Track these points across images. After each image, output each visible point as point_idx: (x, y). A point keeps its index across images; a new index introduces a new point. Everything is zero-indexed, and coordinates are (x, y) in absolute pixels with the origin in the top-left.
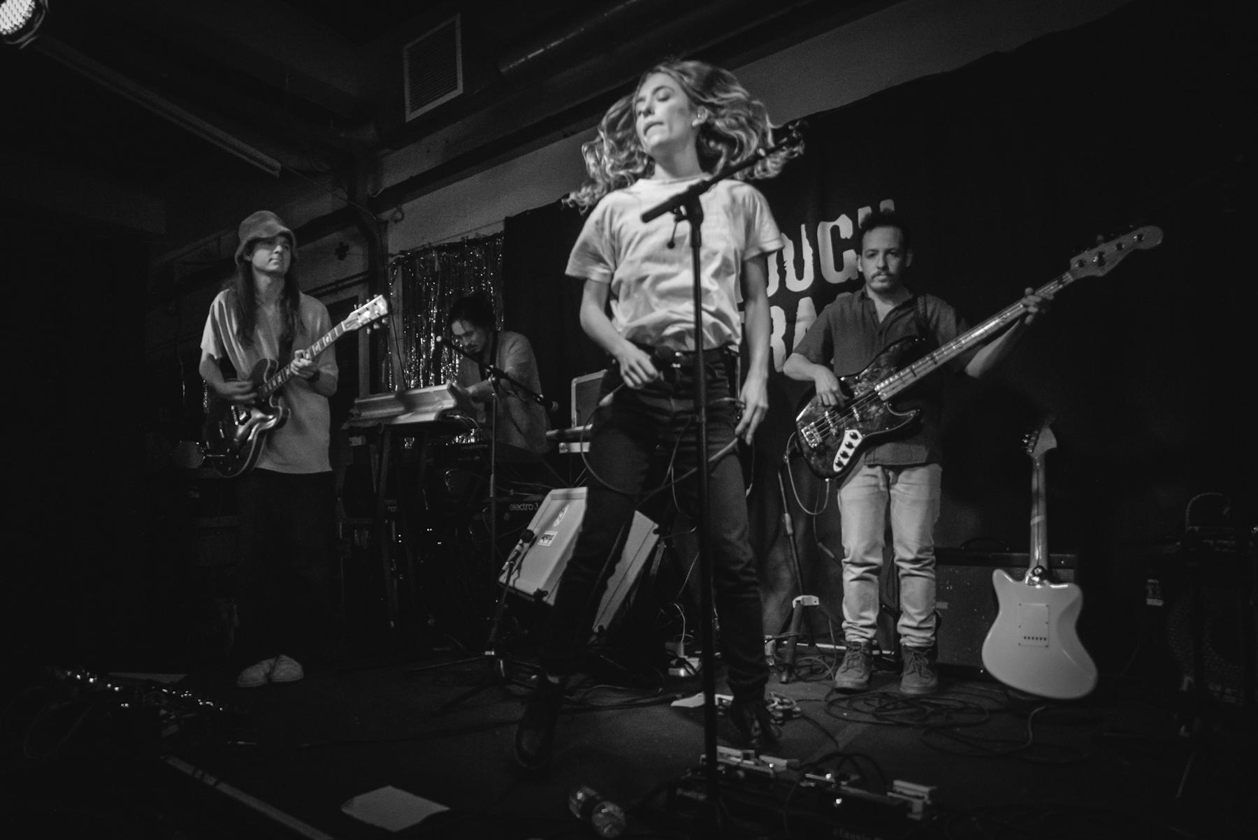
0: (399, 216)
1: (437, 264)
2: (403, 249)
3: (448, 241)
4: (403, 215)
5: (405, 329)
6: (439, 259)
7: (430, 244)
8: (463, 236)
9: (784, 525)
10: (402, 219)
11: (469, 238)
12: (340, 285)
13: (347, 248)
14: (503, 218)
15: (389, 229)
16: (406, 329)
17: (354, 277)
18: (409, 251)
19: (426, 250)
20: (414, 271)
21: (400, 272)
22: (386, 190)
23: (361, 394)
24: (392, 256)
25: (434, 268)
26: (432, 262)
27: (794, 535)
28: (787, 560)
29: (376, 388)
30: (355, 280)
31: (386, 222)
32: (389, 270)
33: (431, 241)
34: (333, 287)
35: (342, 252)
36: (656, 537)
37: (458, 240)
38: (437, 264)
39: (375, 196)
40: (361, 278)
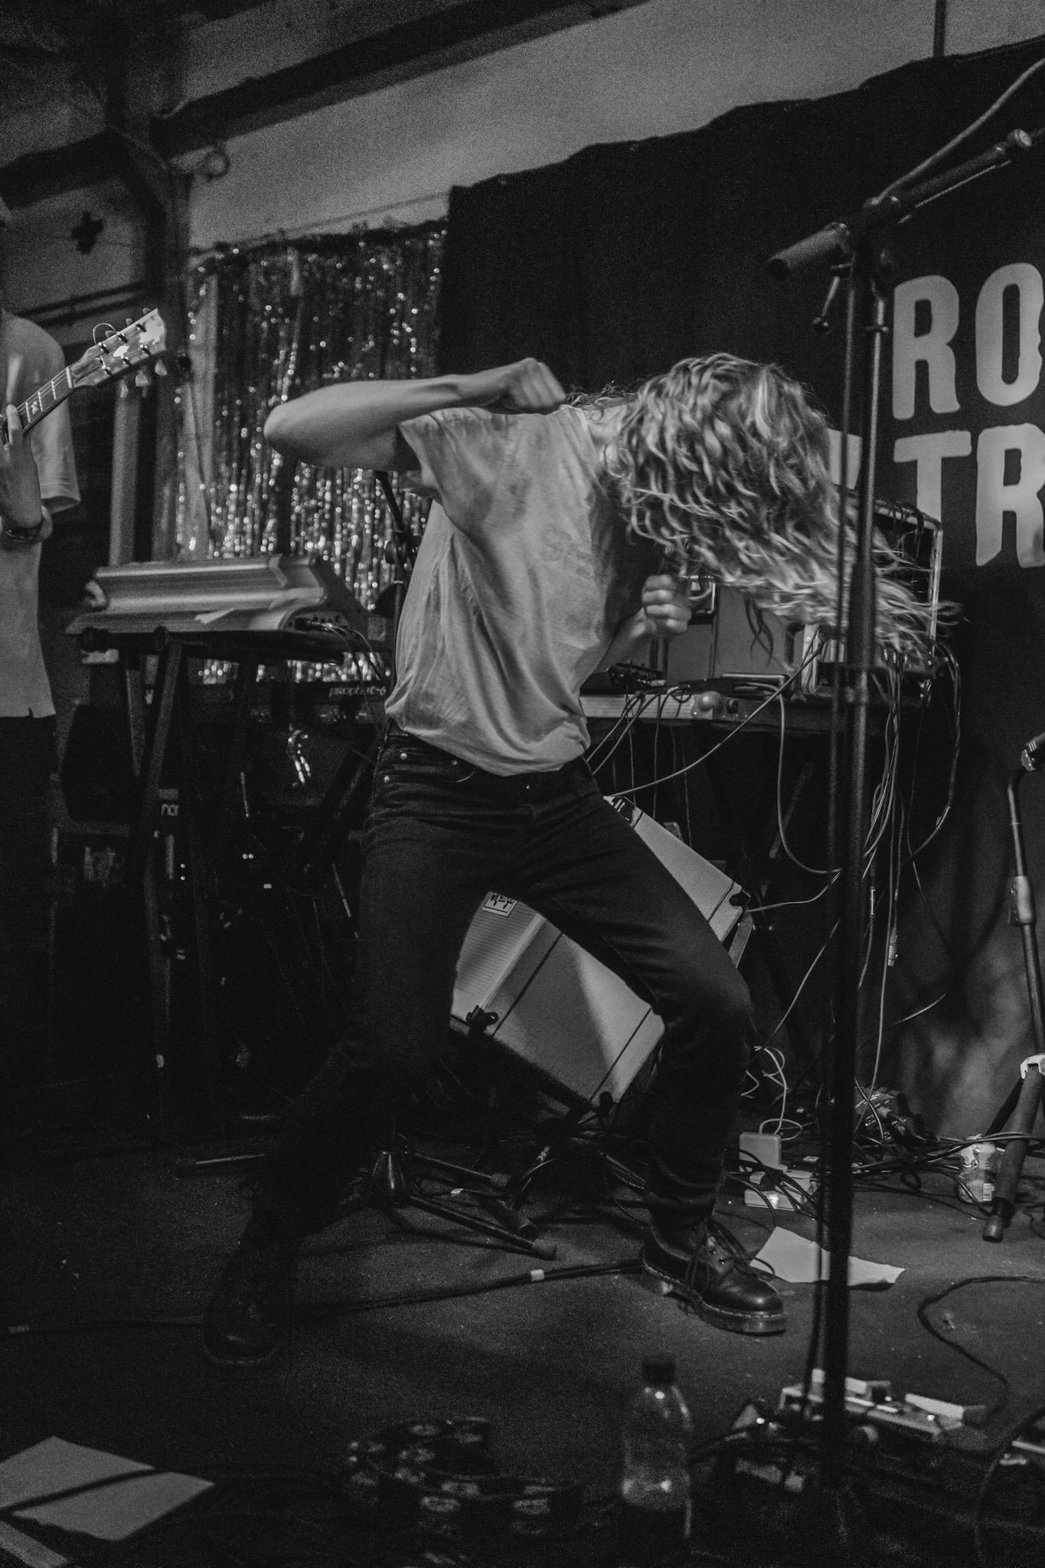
0: (218, 165)
1: (295, 276)
4: (228, 165)
5: (217, 415)
6: (301, 271)
7: (282, 232)
8: (359, 221)
9: (1014, 899)
10: (225, 172)
12: (78, 308)
13: (99, 227)
14: (447, 188)
17: (114, 292)
18: (236, 246)
19: (274, 246)
20: (245, 291)
21: (213, 293)
22: (192, 105)
23: (114, 558)
24: (198, 252)
25: (287, 287)
26: (286, 275)
27: (1033, 923)
28: (1014, 974)
30: (114, 299)
31: (188, 179)
33: (285, 226)
35: (87, 234)
36: (735, 912)
37: (344, 228)
38: (295, 276)
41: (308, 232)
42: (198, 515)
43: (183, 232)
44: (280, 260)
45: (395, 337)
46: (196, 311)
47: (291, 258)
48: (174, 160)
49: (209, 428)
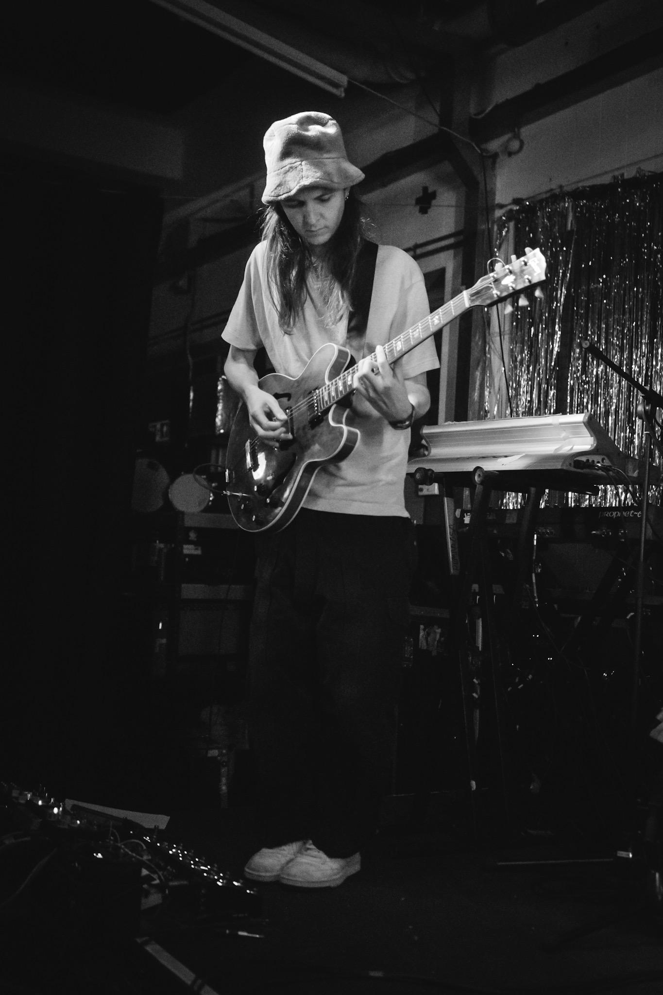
0: (515, 145)
1: (570, 218)
2: (519, 196)
6: (575, 212)
7: (561, 187)
8: (617, 173)
11: (626, 176)
13: (433, 195)
15: (497, 165)
16: (517, 320)
19: (555, 197)
20: (534, 230)
22: (497, 107)
24: (501, 206)
26: (565, 217)
29: (460, 414)
31: (495, 157)
32: (496, 228)
35: (425, 201)
37: (607, 180)
38: (570, 218)
39: (480, 117)
40: (451, 241)
41: (580, 185)
46: (499, 248)
48: (483, 146)
49: (507, 328)
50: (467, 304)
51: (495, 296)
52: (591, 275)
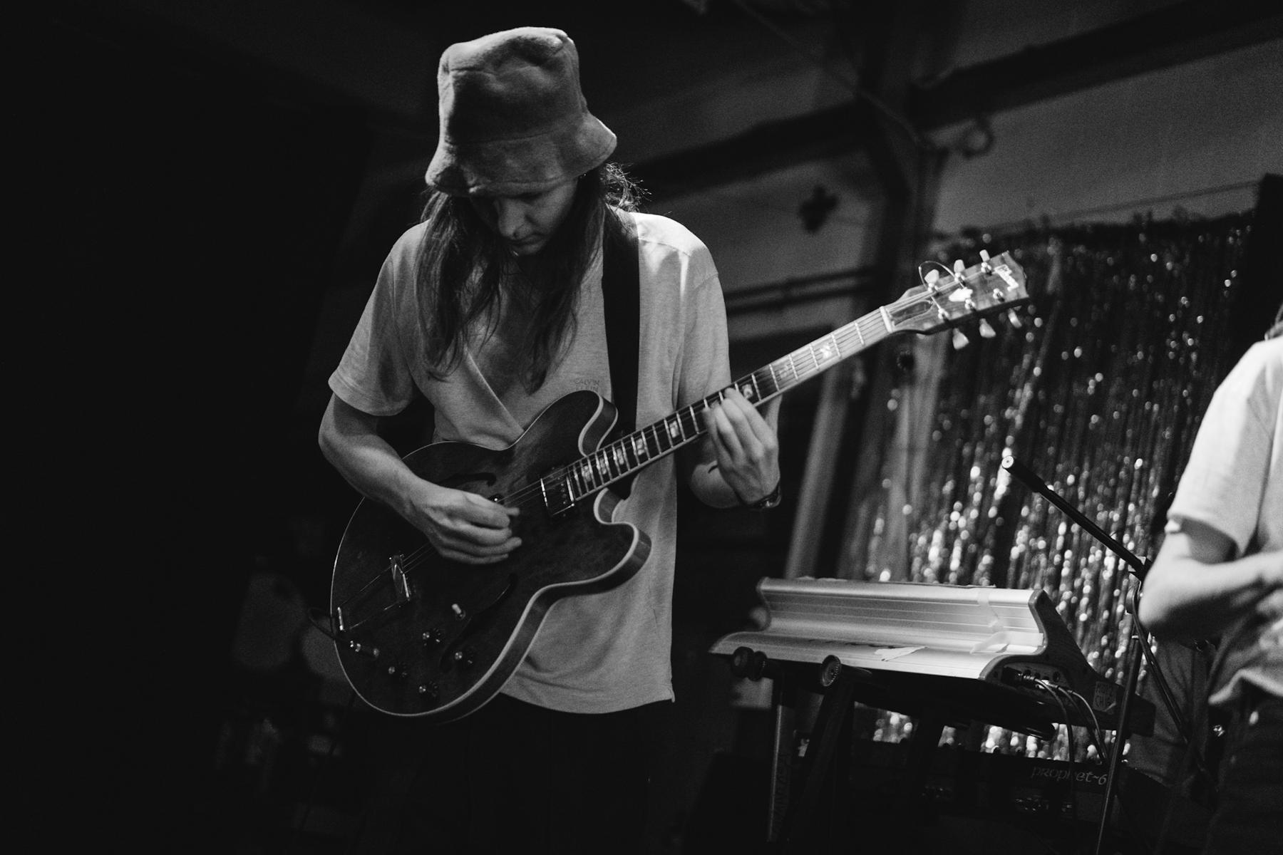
0: (979, 140)
1: (1055, 270)
3: (1096, 219)
4: (991, 140)
5: (936, 425)
6: (1063, 262)
7: (1045, 219)
8: (1143, 211)
24: (942, 237)
30: (834, 285)
31: (942, 155)
33: (1052, 213)
34: (775, 295)
37: (1123, 218)
38: (1055, 270)
40: (850, 283)
41: (1078, 221)
42: (897, 543)
43: (926, 214)
44: (1038, 251)
45: (1171, 349)
47: (1052, 249)
49: (923, 441)
50: (891, 328)
51: (940, 317)
52: (1081, 370)
